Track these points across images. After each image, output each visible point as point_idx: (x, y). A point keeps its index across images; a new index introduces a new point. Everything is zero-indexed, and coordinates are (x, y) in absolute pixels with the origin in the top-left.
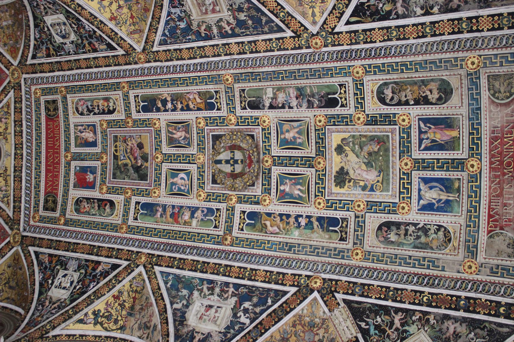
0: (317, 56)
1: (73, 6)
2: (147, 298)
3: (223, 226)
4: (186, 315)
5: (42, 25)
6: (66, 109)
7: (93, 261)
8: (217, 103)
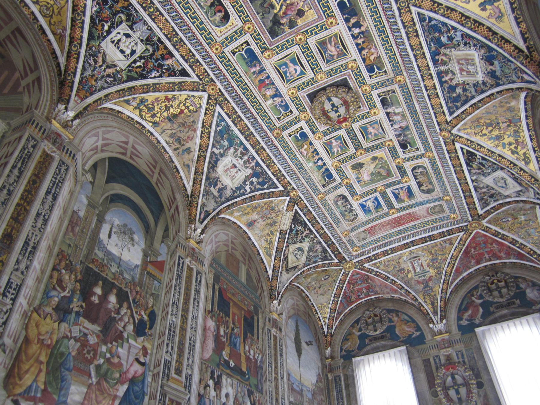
3: (283, 123)
4: (218, 162)
7: (166, 48)
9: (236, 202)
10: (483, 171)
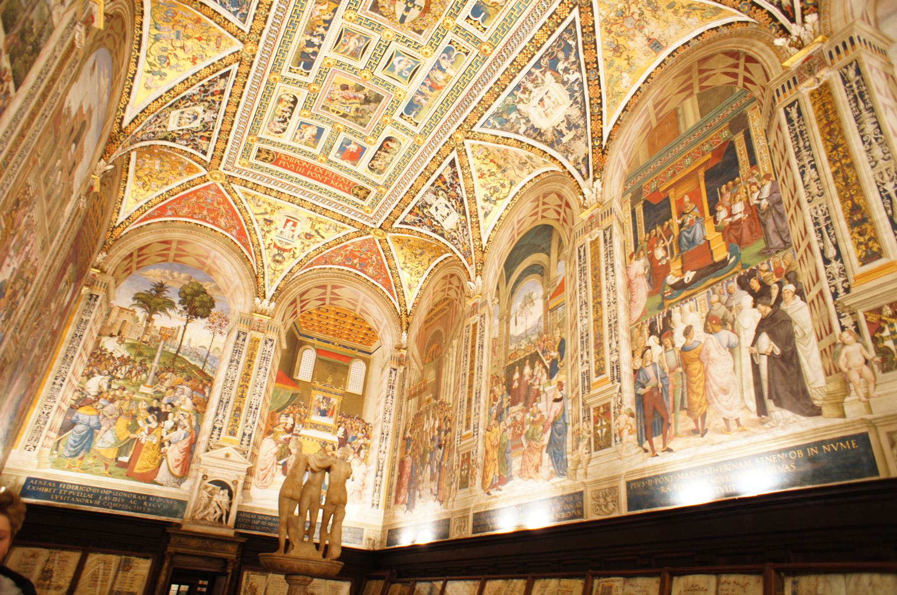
2: (498, 151)
4: (536, 126)
7: (436, 180)
9: (591, 99)
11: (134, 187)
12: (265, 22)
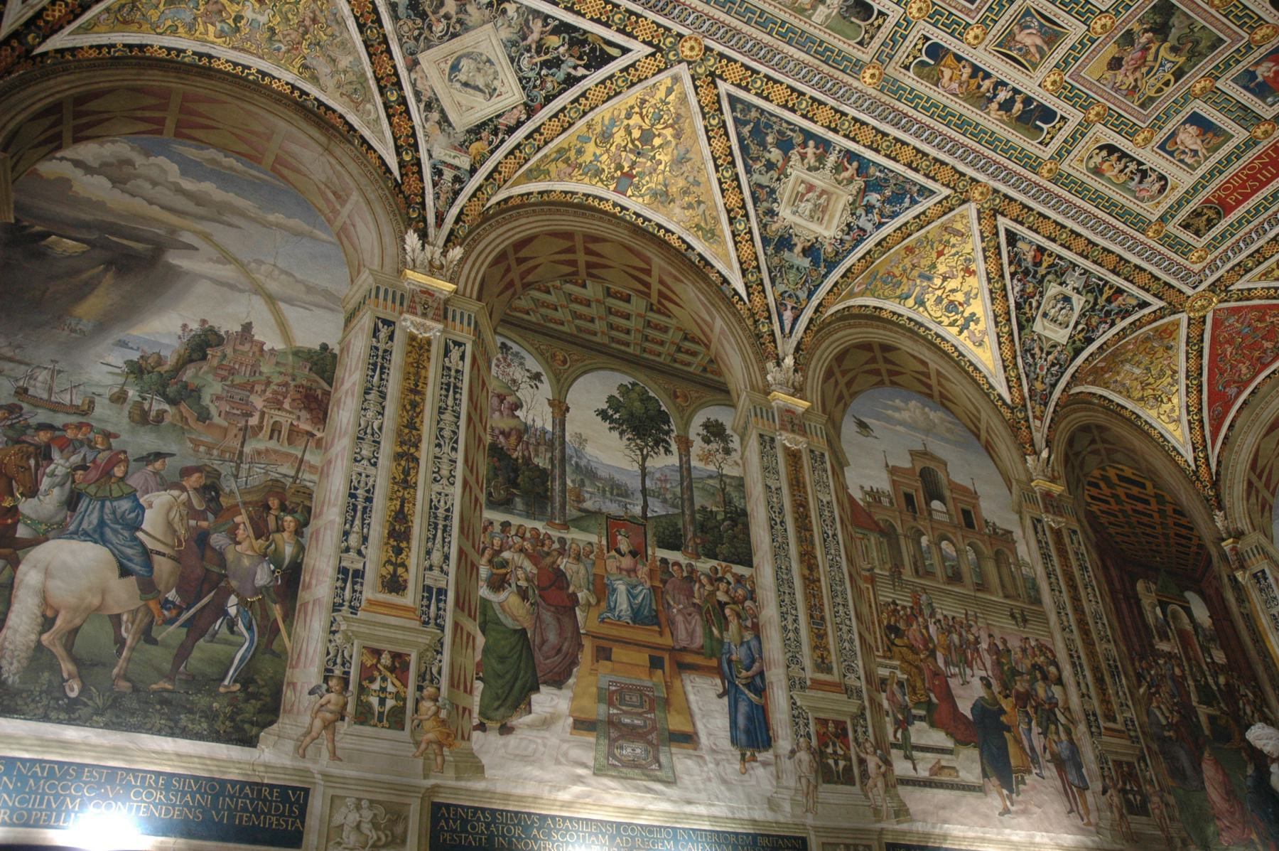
0: (704, 28)
1: (1006, 329)
5: (1081, 336)
6: (1179, 204)
8: (920, 50)
10: (529, 51)
11: (1154, 413)
12: (943, 163)
